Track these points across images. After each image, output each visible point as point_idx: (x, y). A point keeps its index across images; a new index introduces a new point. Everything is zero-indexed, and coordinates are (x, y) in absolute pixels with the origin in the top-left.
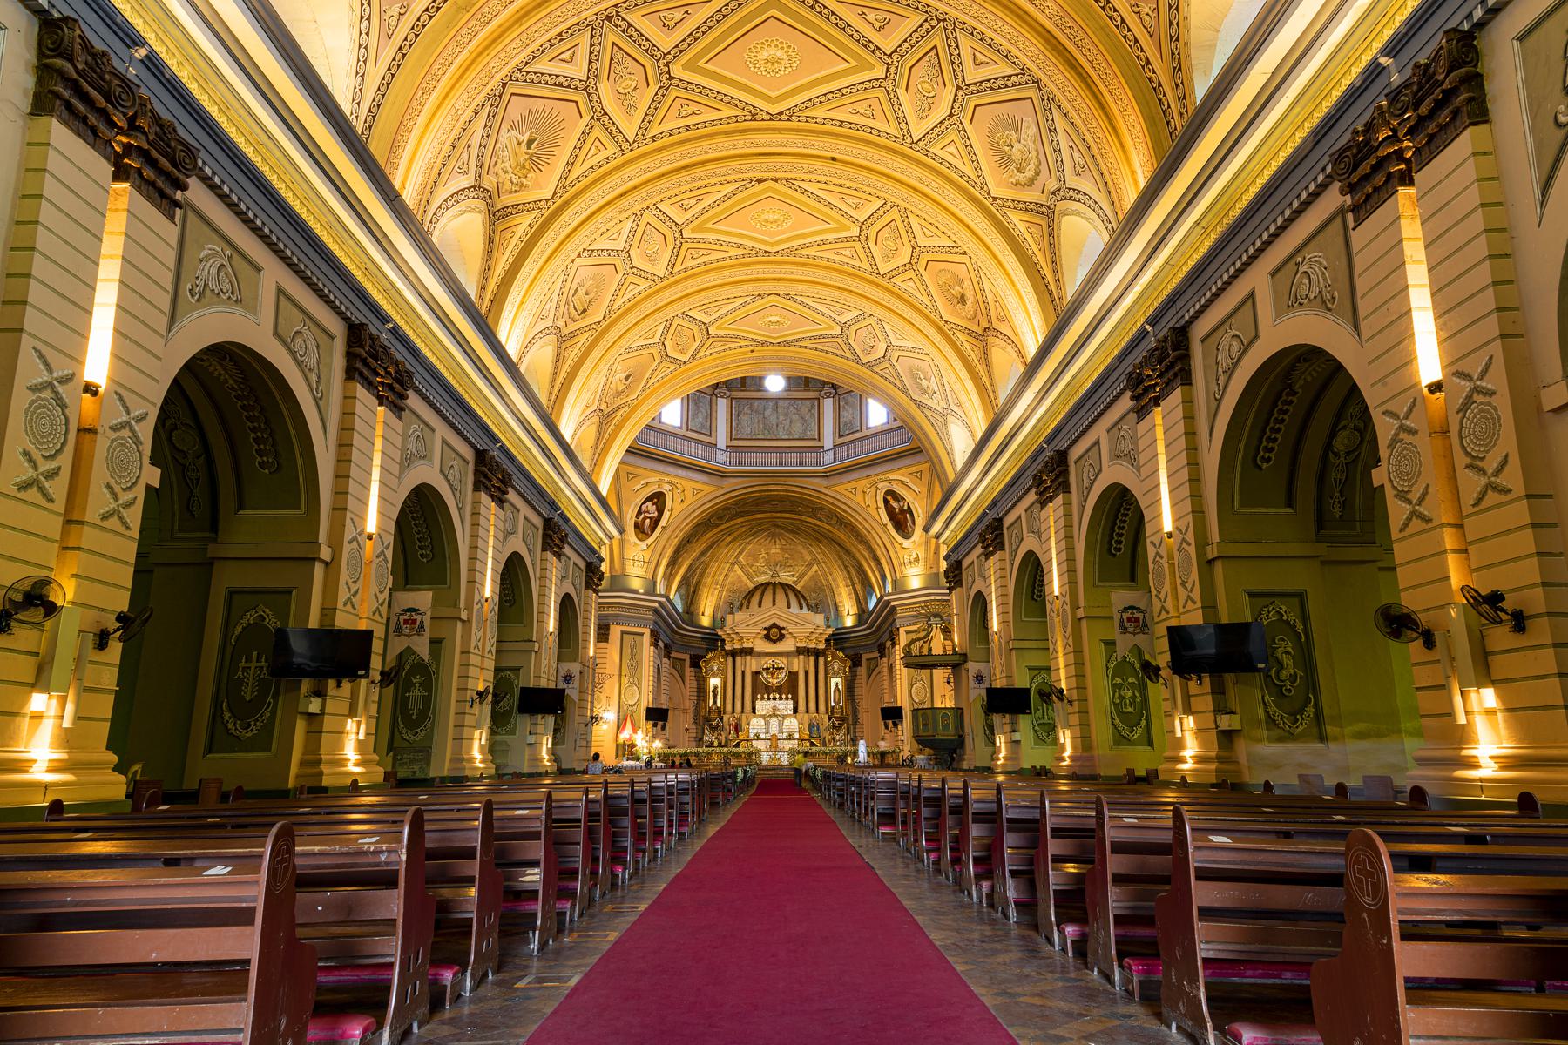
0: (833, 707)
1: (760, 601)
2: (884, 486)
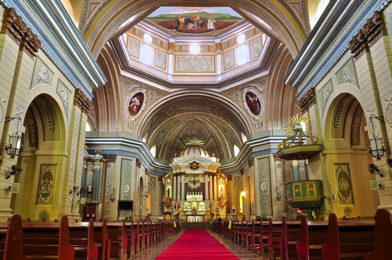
0: (220, 198)
1: (188, 152)
2: (246, 90)
